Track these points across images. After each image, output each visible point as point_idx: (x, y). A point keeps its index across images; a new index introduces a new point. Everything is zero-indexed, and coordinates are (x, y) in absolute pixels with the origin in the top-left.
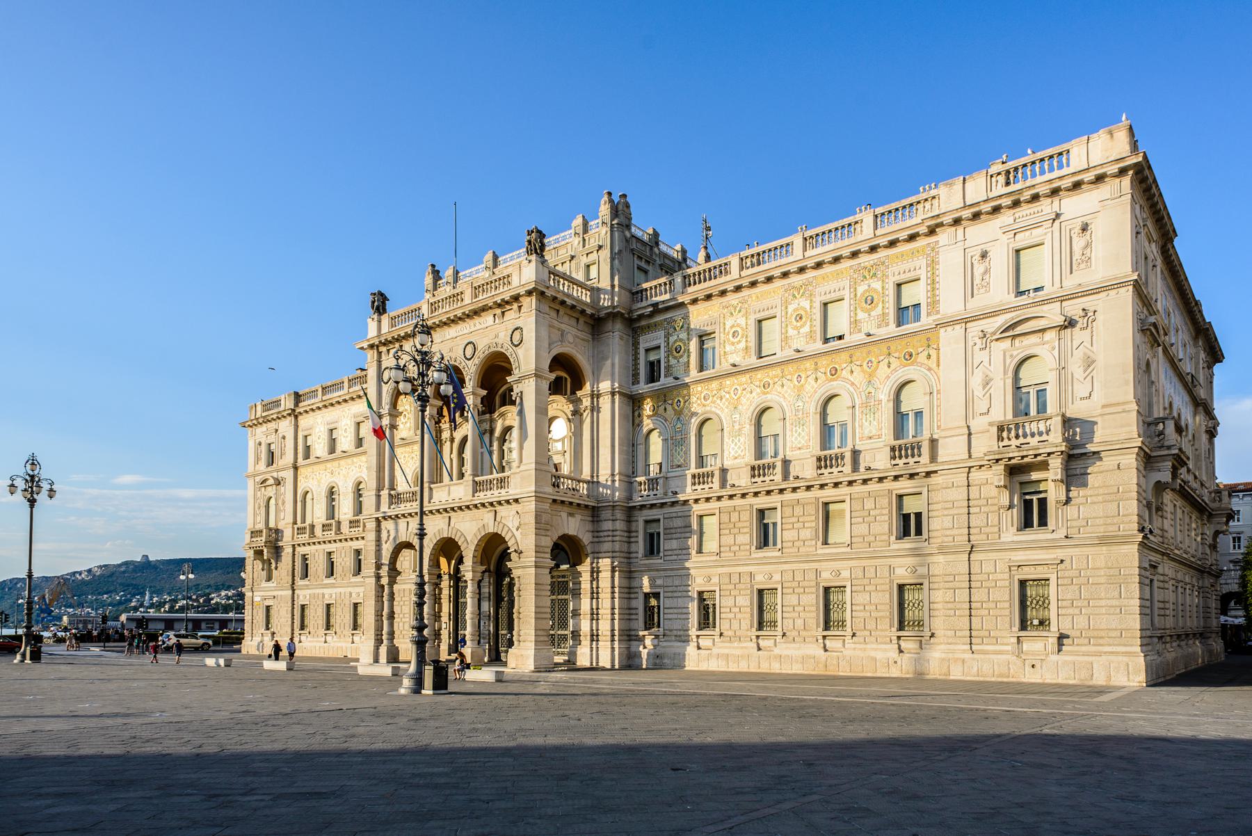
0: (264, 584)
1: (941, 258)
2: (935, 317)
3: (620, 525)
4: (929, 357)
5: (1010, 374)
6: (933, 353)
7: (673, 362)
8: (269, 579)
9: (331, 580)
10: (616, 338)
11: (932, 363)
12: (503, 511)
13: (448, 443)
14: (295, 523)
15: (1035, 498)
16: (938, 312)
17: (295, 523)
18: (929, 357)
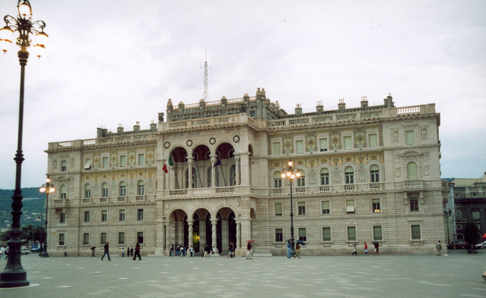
0: (84, 224)
1: (384, 130)
2: (381, 147)
3: (267, 205)
4: (380, 158)
5: (406, 166)
6: (382, 157)
7: (285, 149)
8: (62, 221)
9: (104, 223)
10: (264, 139)
11: (382, 160)
12: (231, 200)
13: (181, 170)
14: (80, 197)
15: (414, 202)
16: (383, 145)
17: (80, 197)
18: (380, 158)
